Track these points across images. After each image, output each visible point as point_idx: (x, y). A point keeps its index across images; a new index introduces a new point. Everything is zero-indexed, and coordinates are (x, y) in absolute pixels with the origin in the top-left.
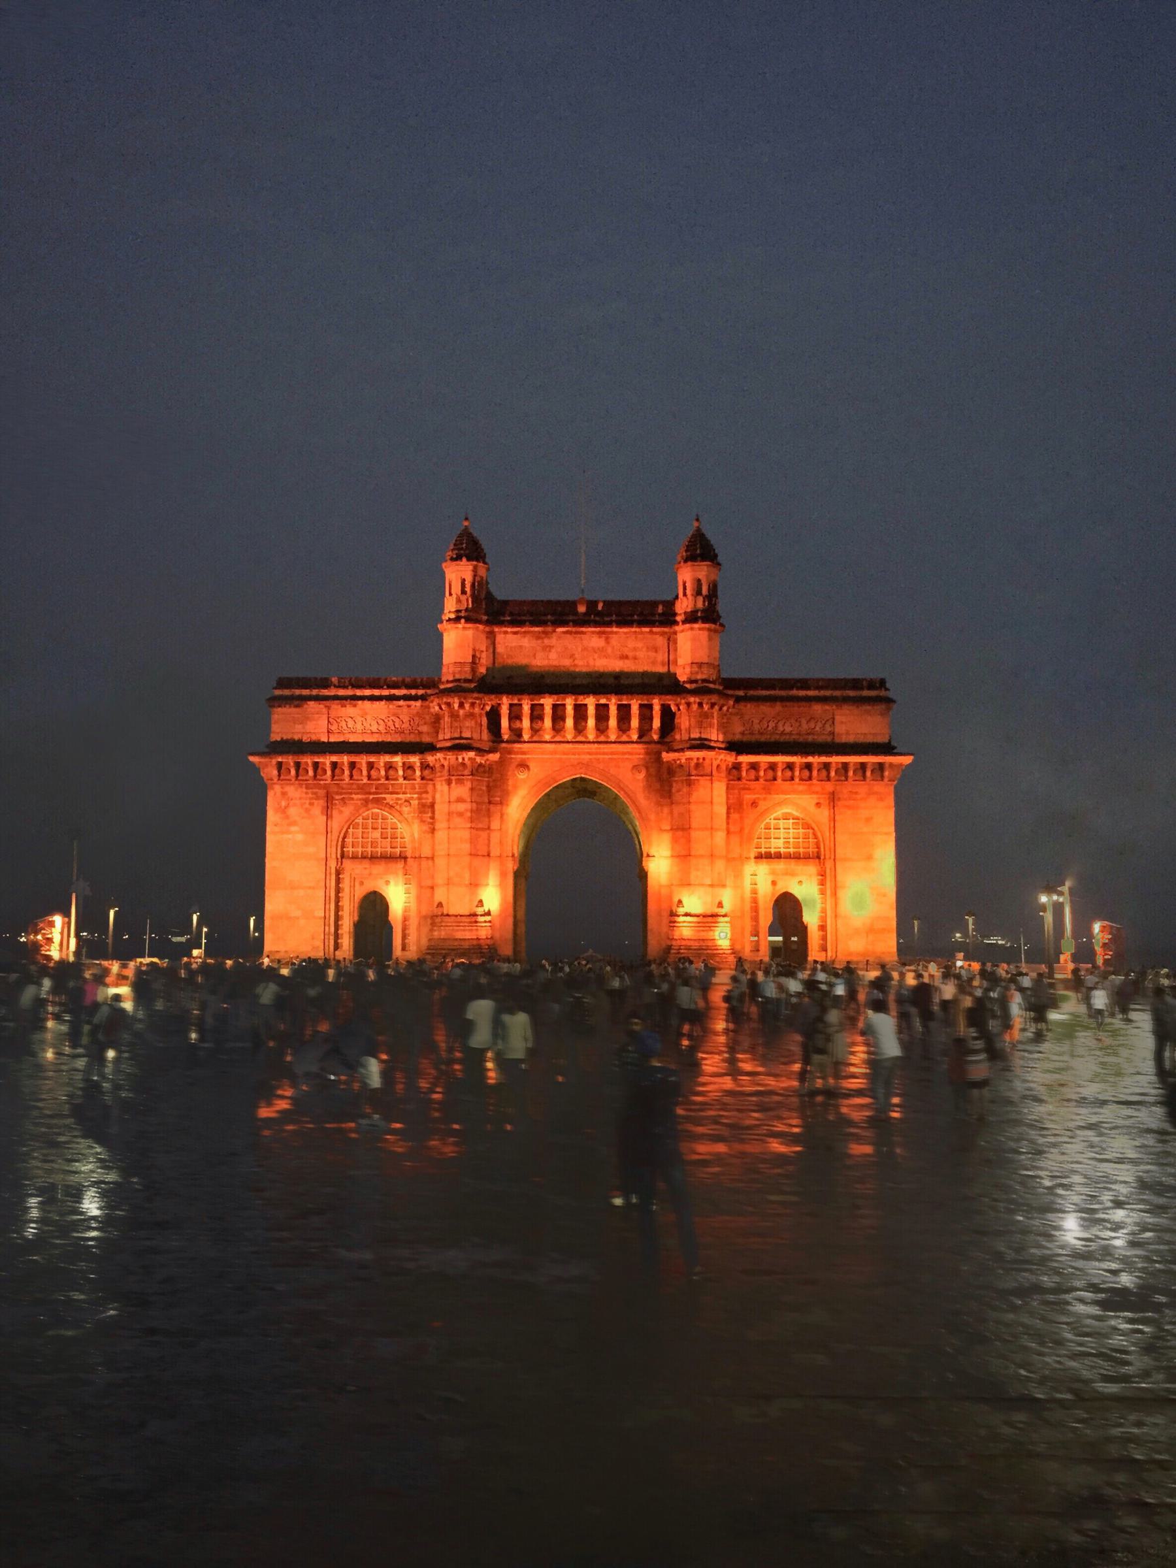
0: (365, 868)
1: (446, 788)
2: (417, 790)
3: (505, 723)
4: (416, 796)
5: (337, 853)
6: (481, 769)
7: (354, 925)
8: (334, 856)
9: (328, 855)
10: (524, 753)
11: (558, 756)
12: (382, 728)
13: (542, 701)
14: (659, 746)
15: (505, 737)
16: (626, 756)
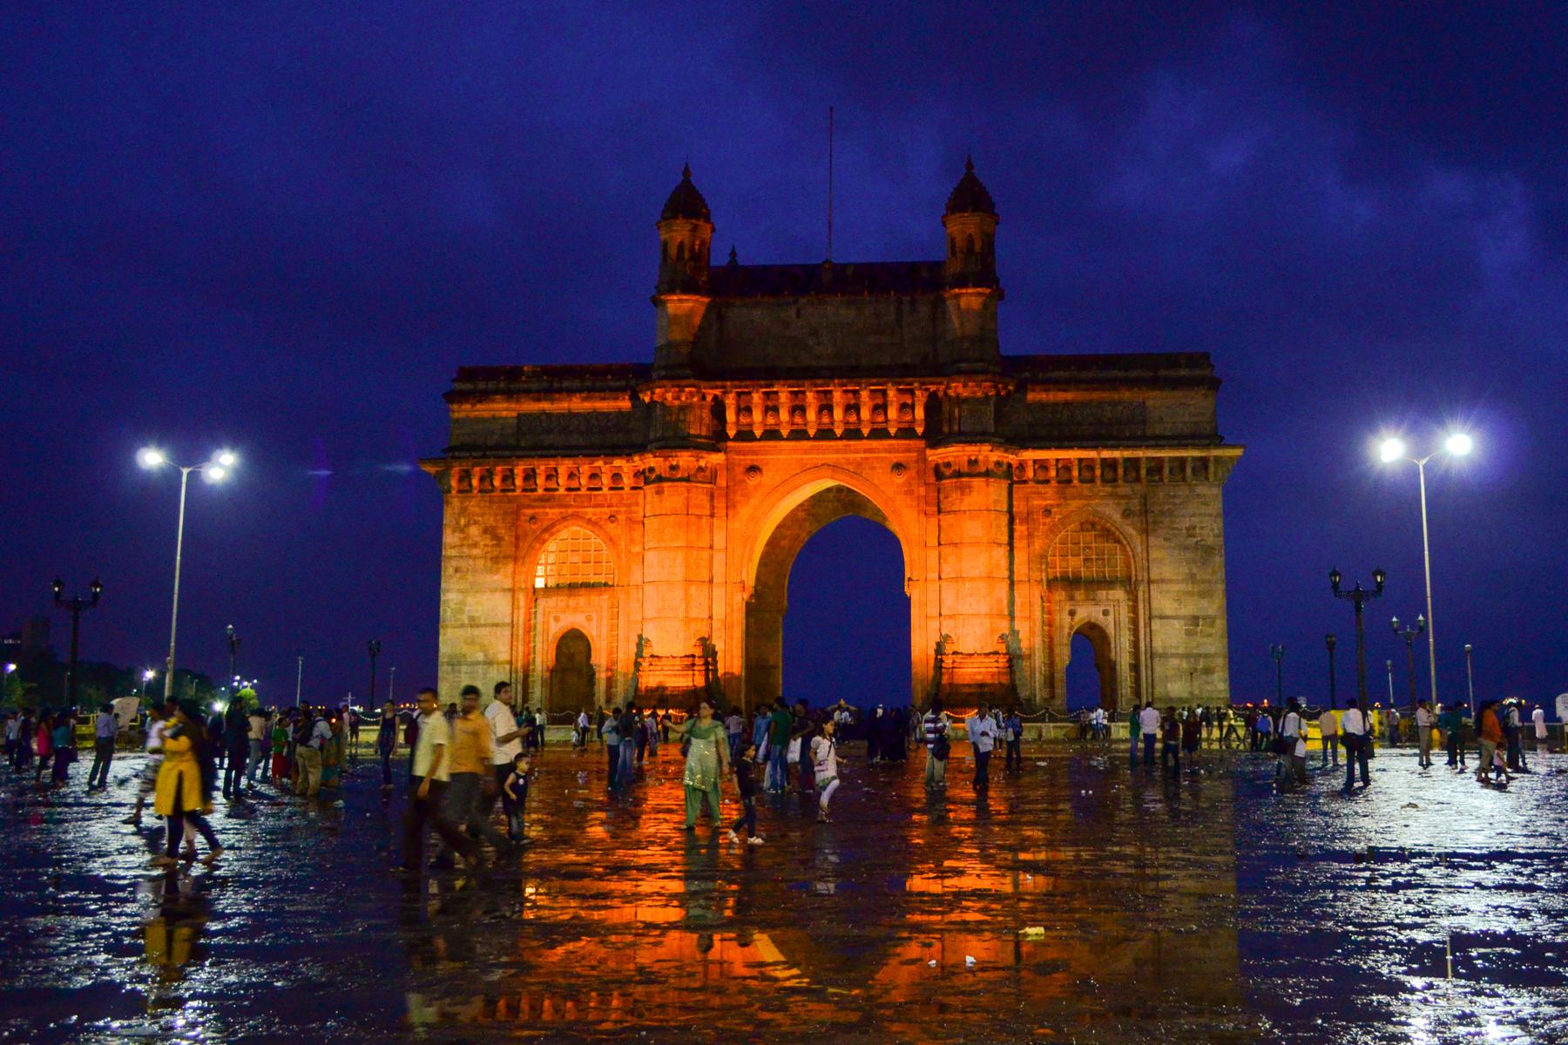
3: (730, 416)
4: (623, 509)
6: (700, 476)
10: (755, 453)
11: (796, 456)
14: (921, 444)
15: (731, 433)
16: (883, 455)
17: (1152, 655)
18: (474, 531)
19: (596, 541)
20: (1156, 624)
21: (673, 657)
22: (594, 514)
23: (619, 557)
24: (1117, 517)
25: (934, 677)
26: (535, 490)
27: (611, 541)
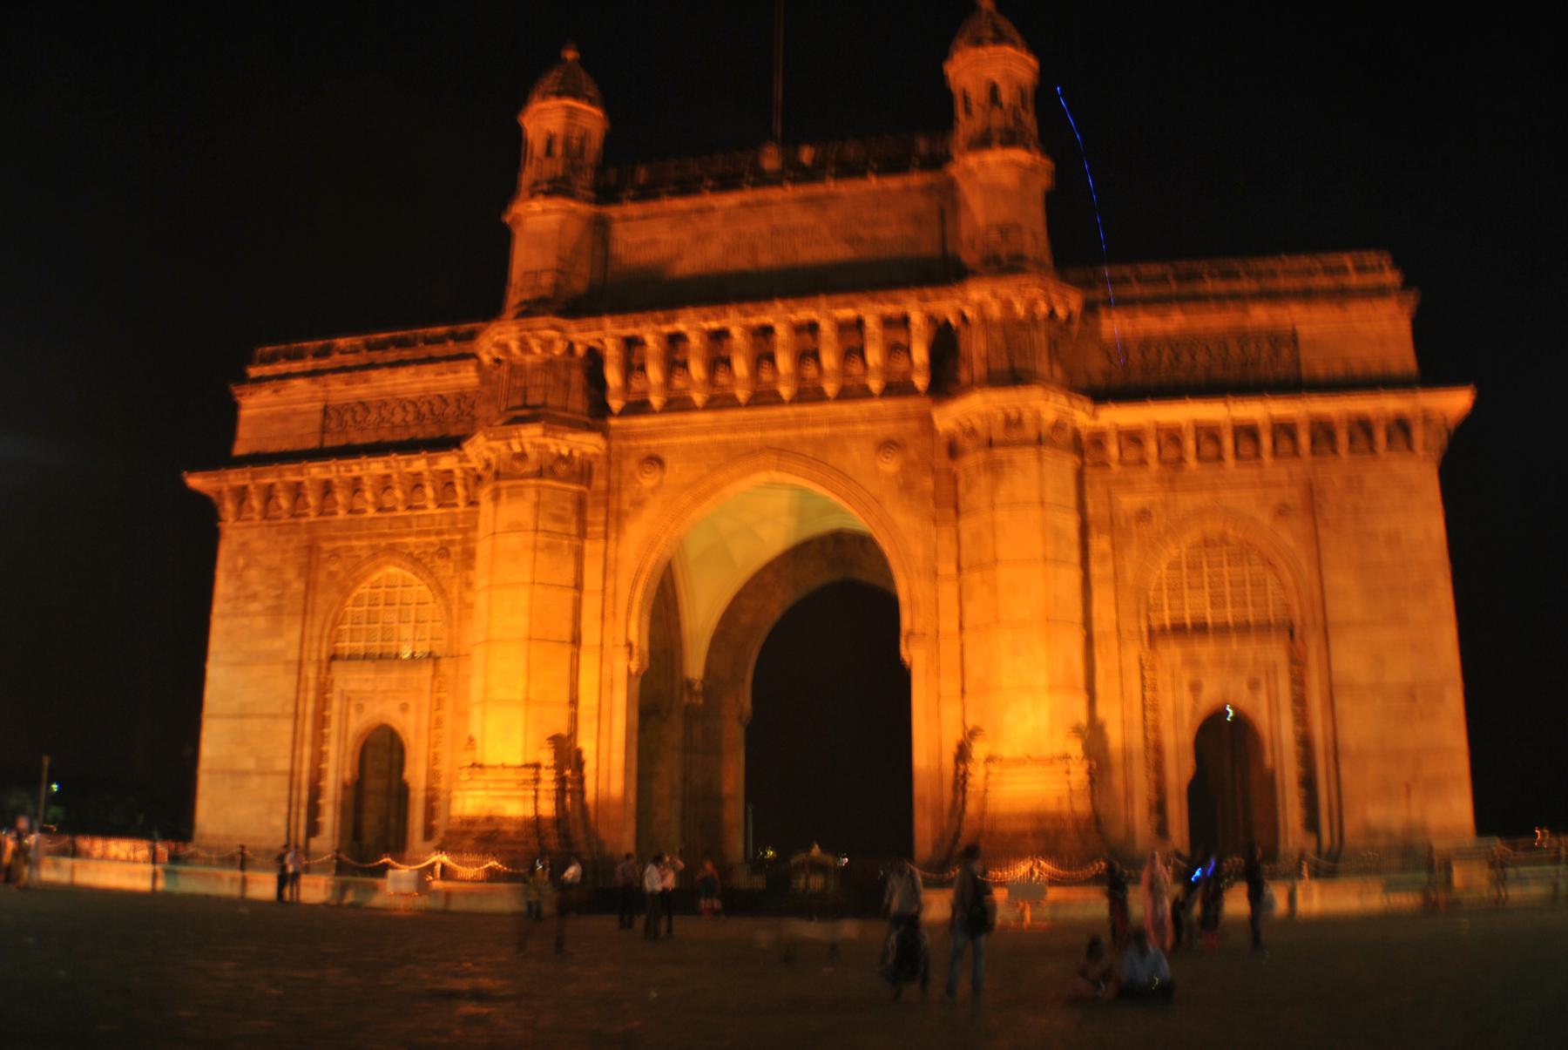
0: (367, 680)
1: (491, 505)
2: (460, 526)
3: (613, 376)
4: (459, 537)
5: (320, 651)
6: (562, 468)
7: (345, 787)
8: (314, 657)
9: (305, 656)
10: (651, 435)
11: (720, 437)
12: (410, 417)
13: (681, 326)
15: (616, 404)
16: (861, 428)
17: (1335, 752)
18: (253, 574)
19: (420, 588)
20: (1343, 704)
21: (504, 766)
22: (417, 547)
23: (449, 610)
24: (1265, 518)
25: (954, 802)
26: (334, 513)
27: (440, 590)
